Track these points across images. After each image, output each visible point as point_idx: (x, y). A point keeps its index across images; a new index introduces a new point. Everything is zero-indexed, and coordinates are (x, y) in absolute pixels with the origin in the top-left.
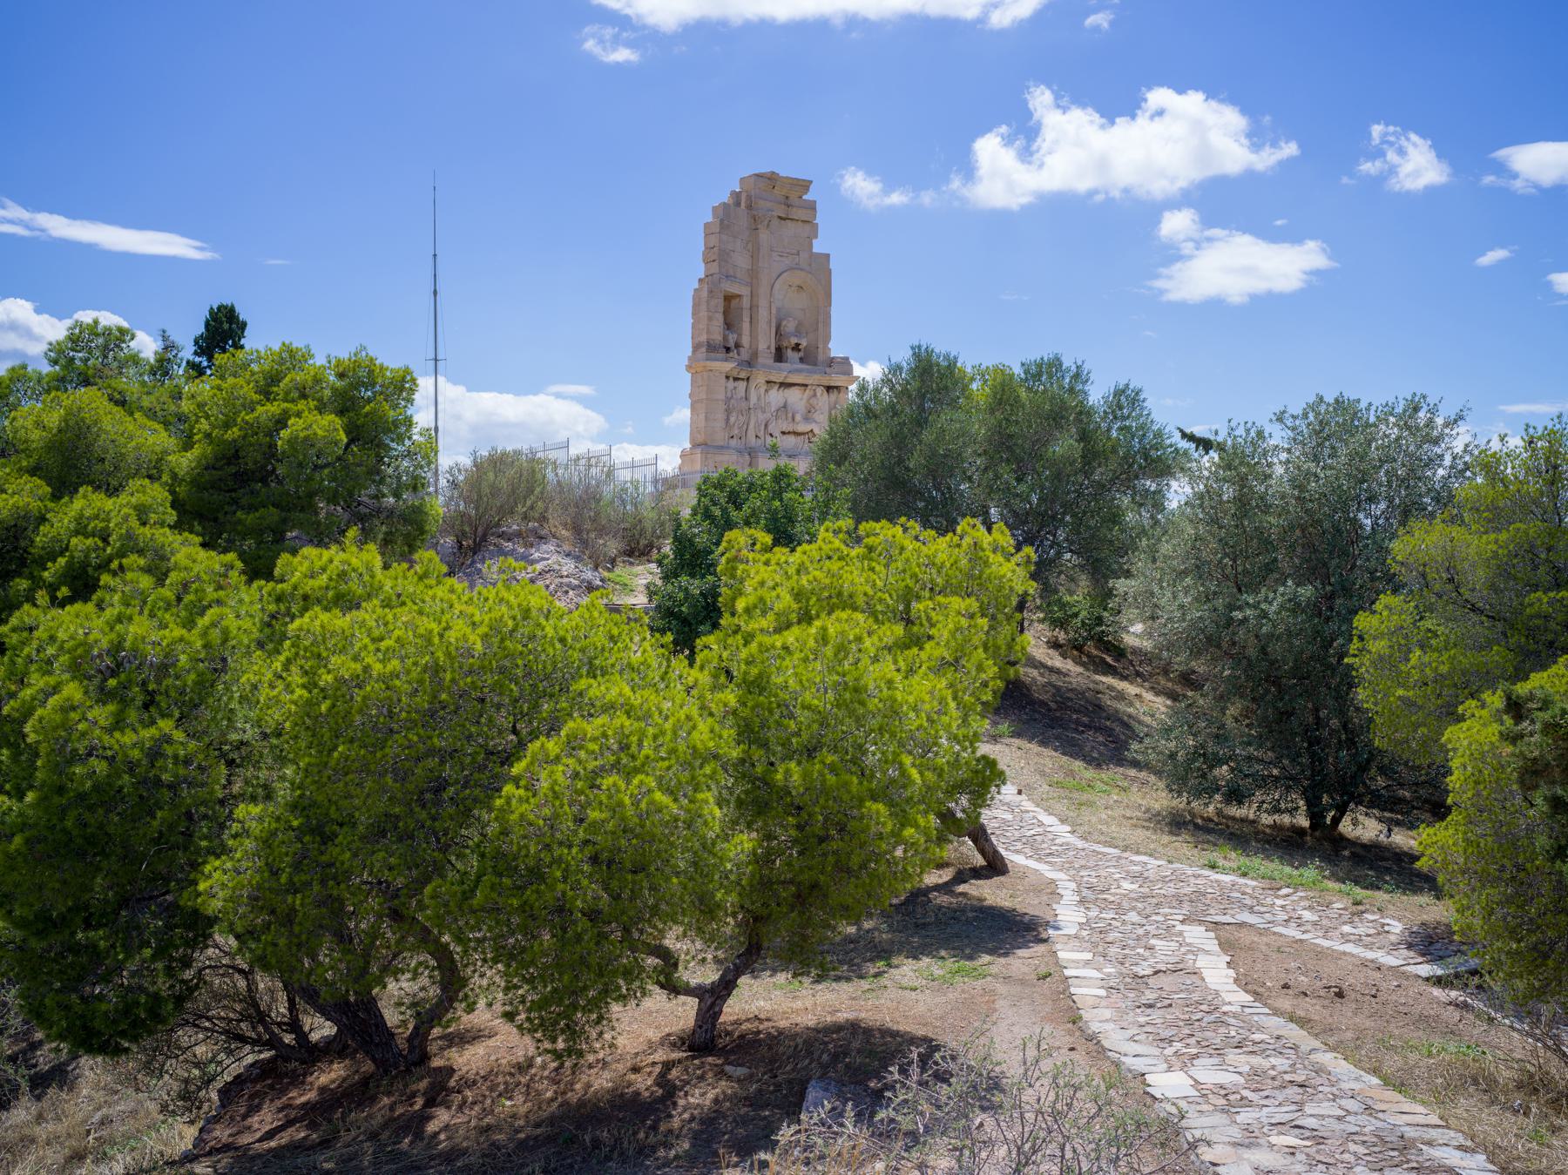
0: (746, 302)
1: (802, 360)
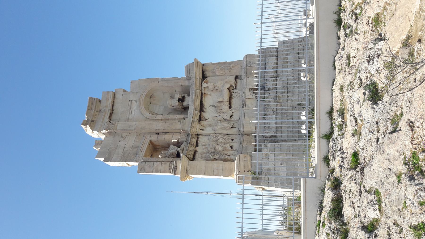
0: (154, 138)
1: (189, 95)
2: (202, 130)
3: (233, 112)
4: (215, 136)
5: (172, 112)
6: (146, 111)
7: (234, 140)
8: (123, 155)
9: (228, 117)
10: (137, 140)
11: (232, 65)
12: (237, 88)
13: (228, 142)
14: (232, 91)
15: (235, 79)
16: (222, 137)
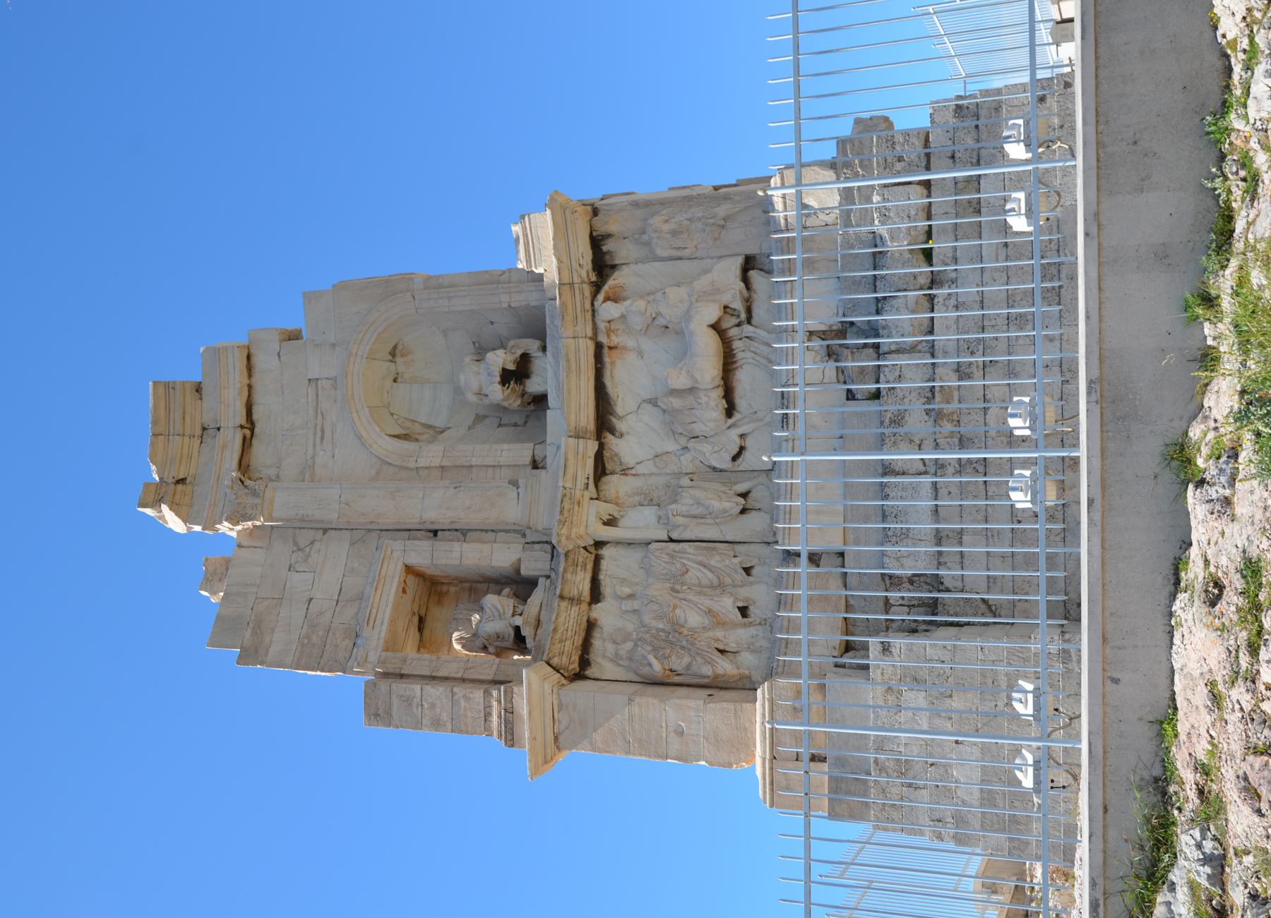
0: (422, 555)
2: (611, 522)
3: (742, 436)
4: (668, 554)
5: (485, 417)
6: (378, 429)
7: (754, 572)
8: (308, 636)
9: (723, 461)
10: (356, 565)
11: (723, 210)
12: (754, 315)
13: (728, 580)
14: (733, 332)
15: (746, 280)
16: (700, 558)
